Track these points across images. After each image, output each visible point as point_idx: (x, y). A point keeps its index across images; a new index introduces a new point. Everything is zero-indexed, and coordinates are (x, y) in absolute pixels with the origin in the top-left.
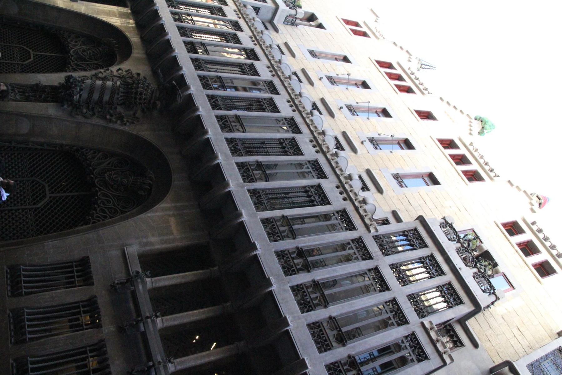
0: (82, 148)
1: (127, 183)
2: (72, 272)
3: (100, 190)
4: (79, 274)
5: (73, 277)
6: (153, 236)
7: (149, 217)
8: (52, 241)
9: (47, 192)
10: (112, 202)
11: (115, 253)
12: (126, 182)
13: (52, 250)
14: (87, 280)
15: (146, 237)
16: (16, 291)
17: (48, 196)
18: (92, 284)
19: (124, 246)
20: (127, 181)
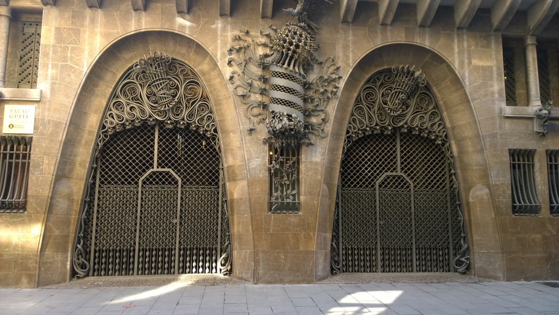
0: (348, 132)
1: (405, 94)
2: (524, 165)
3: (406, 123)
4: (521, 159)
5: (519, 165)
6: (492, 86)
7: (470, 84)
8: (491, 178)
9: (394, 173)
10: (422, 115)
11: (507, 125)
12: (403, 95)
13: (501, 179)
14: (529, 154)
15: (493, 93)
16: (535, 210)
17: (399, 173)
18: (535, 150)
19: (501, 116)
20: (402, 94)
